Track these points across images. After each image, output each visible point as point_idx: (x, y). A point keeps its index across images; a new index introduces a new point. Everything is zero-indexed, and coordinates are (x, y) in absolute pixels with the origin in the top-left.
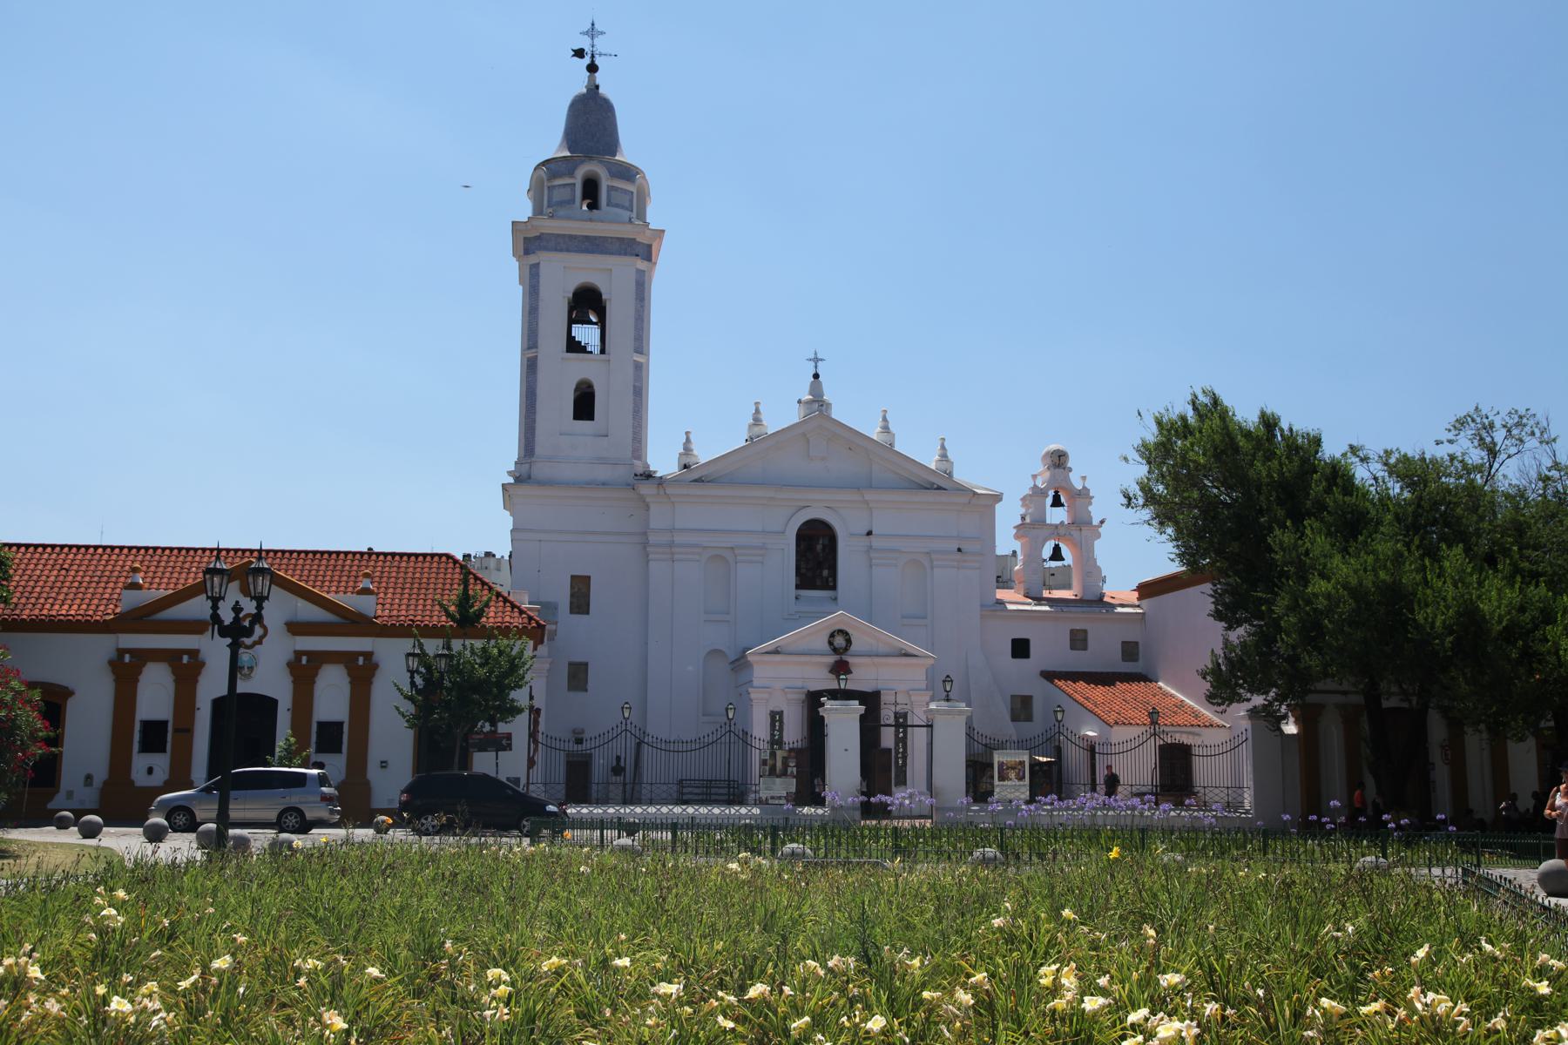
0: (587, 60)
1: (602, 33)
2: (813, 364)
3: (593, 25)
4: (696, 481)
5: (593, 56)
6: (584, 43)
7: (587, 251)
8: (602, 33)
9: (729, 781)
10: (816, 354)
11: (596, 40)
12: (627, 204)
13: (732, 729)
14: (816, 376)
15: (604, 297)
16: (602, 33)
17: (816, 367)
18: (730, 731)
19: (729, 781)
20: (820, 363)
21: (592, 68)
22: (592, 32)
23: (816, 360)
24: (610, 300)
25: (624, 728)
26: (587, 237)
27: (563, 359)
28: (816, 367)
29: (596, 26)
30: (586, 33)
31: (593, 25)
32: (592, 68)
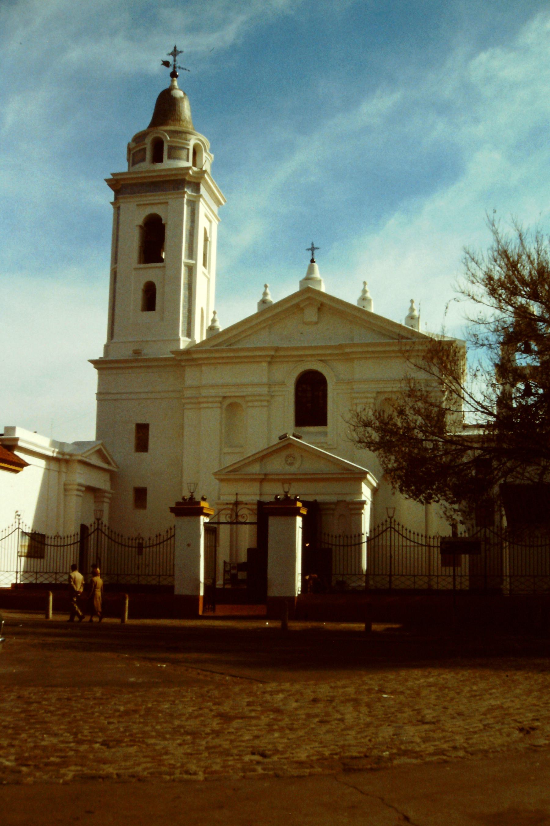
0: (171, 70)
1: (181, 52)
2: (310, 252)
3: (175, 48)
5: (175, 67)
9: (430, 575)
10: (313, 245)
11: (177, 58)
13: (100, 527)
14: (312, 261)
15: (163, 222)
17: (313, 254)
18: (98, 529)
19: (390, 576)
20: (316, 252)
21: (174, 75)
23: (313, 249)
24: (167, 223)
25: (17, 527)
27: (135, 269)
28: (313, 254)
29: (178, 49)
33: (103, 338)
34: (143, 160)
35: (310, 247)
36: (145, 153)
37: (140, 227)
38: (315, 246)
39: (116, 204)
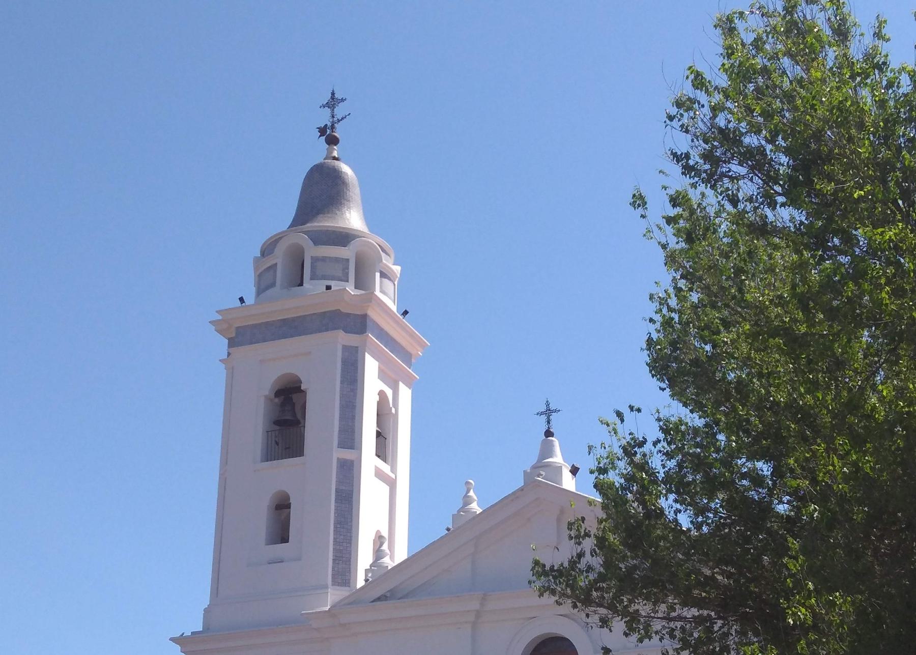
2: (544, 417)
3: (333, 94)
4: (379, 599)
6: (324, 118)
7: (284, 336)
8: (343, 100)
10: (548, 404)
12: (340, 274)
14: (548, 434)
16: (343, 100)
17: (549, 422)
20: (554, 417)
22: (333, 102)
23: (548, 412)
26: (284, 321)
28: (549, 422)
30: (327, 105)
31: (333, 94)
32: (332, 141)
33: (204, 599)
34: (273, 285)
35: (543, 409)
36: (275, 272)
37: (266, 397)
38: (552, 407)
39: (228, 361)
